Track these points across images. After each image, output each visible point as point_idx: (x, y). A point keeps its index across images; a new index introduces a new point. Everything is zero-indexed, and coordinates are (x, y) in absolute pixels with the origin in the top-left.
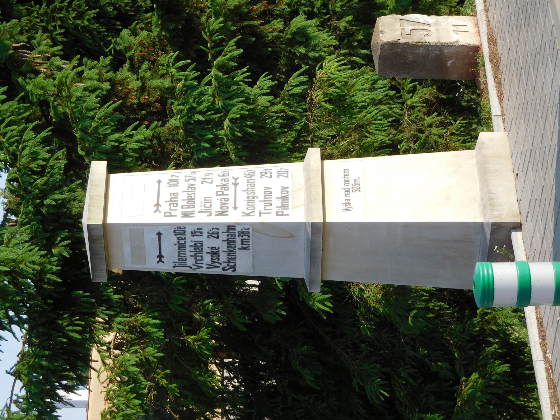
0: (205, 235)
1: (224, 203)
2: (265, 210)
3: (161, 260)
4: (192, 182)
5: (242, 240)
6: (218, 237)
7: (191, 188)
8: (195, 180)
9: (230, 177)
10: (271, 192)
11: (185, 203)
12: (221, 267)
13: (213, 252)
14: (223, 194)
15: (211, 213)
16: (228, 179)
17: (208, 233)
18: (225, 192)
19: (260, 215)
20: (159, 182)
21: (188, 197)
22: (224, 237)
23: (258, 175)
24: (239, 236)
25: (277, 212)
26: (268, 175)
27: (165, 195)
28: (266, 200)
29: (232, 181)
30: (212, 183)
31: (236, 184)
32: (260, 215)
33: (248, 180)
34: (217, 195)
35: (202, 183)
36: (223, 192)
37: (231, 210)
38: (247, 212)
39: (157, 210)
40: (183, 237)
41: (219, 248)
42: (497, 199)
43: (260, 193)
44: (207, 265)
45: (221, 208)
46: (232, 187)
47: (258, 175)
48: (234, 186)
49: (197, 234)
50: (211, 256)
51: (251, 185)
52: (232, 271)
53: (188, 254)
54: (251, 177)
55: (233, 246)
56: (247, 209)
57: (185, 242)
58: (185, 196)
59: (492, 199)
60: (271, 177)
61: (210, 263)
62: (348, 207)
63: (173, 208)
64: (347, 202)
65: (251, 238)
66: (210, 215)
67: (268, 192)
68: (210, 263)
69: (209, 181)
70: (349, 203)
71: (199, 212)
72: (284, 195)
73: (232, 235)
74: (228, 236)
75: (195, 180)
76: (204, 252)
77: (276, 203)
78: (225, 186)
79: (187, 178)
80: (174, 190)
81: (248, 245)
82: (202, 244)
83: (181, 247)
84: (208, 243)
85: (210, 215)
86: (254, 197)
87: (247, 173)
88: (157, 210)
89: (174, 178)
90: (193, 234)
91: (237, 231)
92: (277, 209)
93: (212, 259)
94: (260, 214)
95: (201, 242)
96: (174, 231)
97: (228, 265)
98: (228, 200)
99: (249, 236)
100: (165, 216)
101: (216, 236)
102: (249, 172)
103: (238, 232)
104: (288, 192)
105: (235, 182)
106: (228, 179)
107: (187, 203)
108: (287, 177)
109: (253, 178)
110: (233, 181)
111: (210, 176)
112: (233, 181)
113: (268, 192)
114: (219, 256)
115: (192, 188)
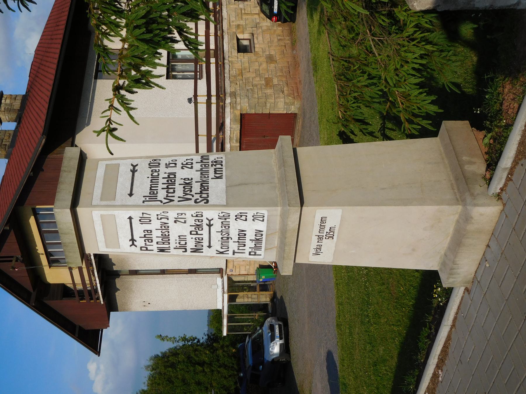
0: (179, 165)
1: (199, 242)
2: (239, 249)
3: (134, 167)
4: (164, 220)
5: (215, 169)
6: (192, 168)
7: (165, 226)
8: (168, 219)
9: (204, 218)
10: (245, 235)
11: (160, 240)
12: (193, 199)
13: (187, 184)
14: (197, 234)
15: (186, 249)
16: (202, 220)
17: (182, 164)
18: (199, 232)
19: (234, 254)
20: (130, 218)
21: (162, 235)
22: (197, 166)
23: (232, 217)
24: (212, 166)
25: (250, 252)
26: (244, 218)
27: (139, 230)
28: (240, 241)
29: (206, 222)
30: (185, 222)
31: (210, 225)
32: (234, 254)
33: (222, 222)
34: (191, 234)
35: (175, 222)
36: (197, 232)
37: (205, 248)
38: (222, 250)
39: (133, 244)
40: (157, 169)
41: (192, 179)
42: (458, 269)
43: (234, 234)
44: (179, 197)
45: (196, 246)
46: (206, 228)
47: (232, 217)
48: (208, 227)
49: (171, 165)
50: (184, 187)
51: (225, 227)
52: (205, 203)
53: (160, 186)
54: (225, 219)
55: (206, 176)
56: (221, 248)
57: (159, 175)
58: (159, 233)
59: (454, 269)
60: (246, 220)
61: (182, 195)
62: (318, 251)
63: (148, 243)
64: (318, 247)
65: (224, 167)
66: (186, 251)
67: (242, 234)
68: (182, 195)
69: (183, 220)
70: (320, 249)
71: (174, 248)
72: (258, 238)
73: (205, 165)
74: (201, 166)
75: (168, 219)
76: (177, 183)
77: (250, 244)
78: (199, 227)
79: (160, 217)
80: (147, 227)
81: (222, 173)
82: (175, 176)
83: (154, 179)
84: (182, 174)
85: (186, 251)
86: (228, 238)
87: (222, 215)
88: (133, 244)
89: (145, 216)
90: (167, 166)
91: (210, 161)
92: (250, 250)
93: (184, 191)
94: (234, 253)
95: (174, 174)
96: (149, 164)
97: (201, 197)
98: (202, 239)
99: (222, 165)
100: (141, 250)
101: (190, 166)
102: (224, 214)
103: (212, 162)
104: (262, 235)
105: (210, 223)
106: (202, 220)
107: (162, 239)
108: (263, 221)
109: (228, 220)
110: (208, 222)
111: (183, 216)
112: (208, 222)
113: (242, 234)
114: (192, 187)
115: (165, 227)
